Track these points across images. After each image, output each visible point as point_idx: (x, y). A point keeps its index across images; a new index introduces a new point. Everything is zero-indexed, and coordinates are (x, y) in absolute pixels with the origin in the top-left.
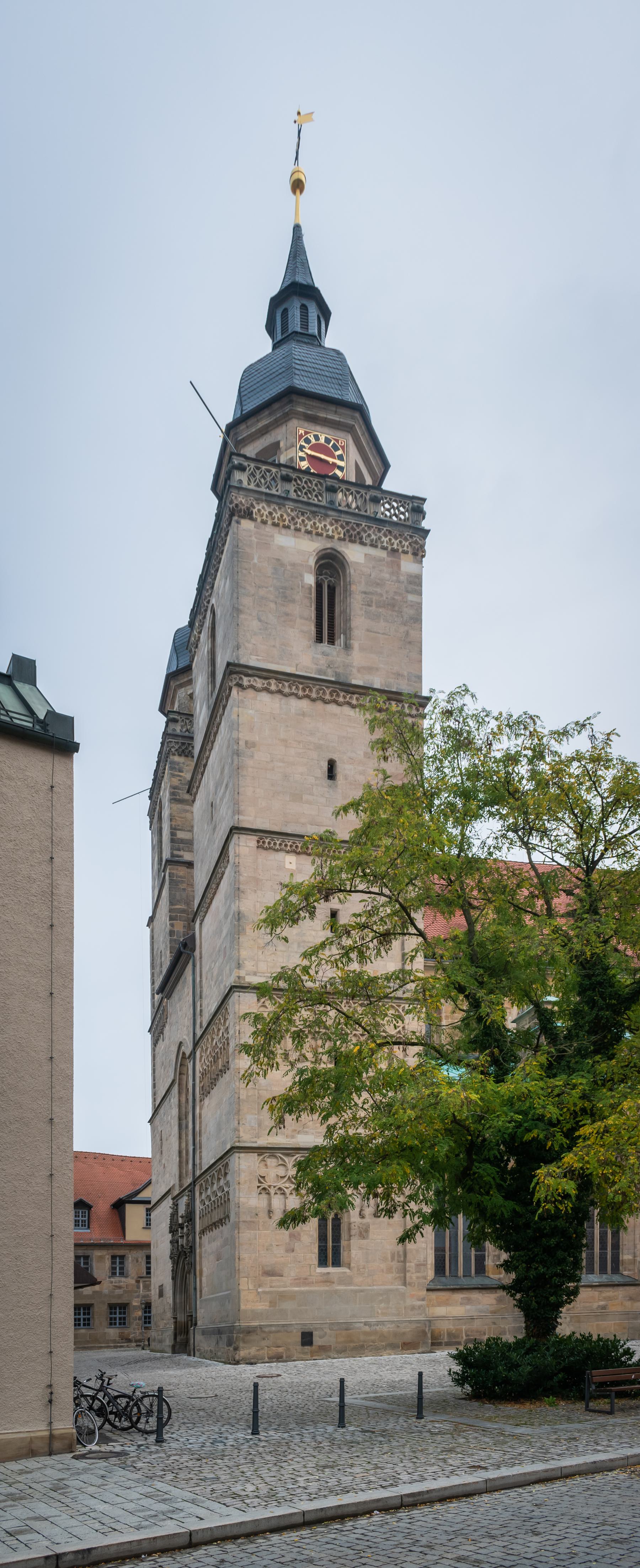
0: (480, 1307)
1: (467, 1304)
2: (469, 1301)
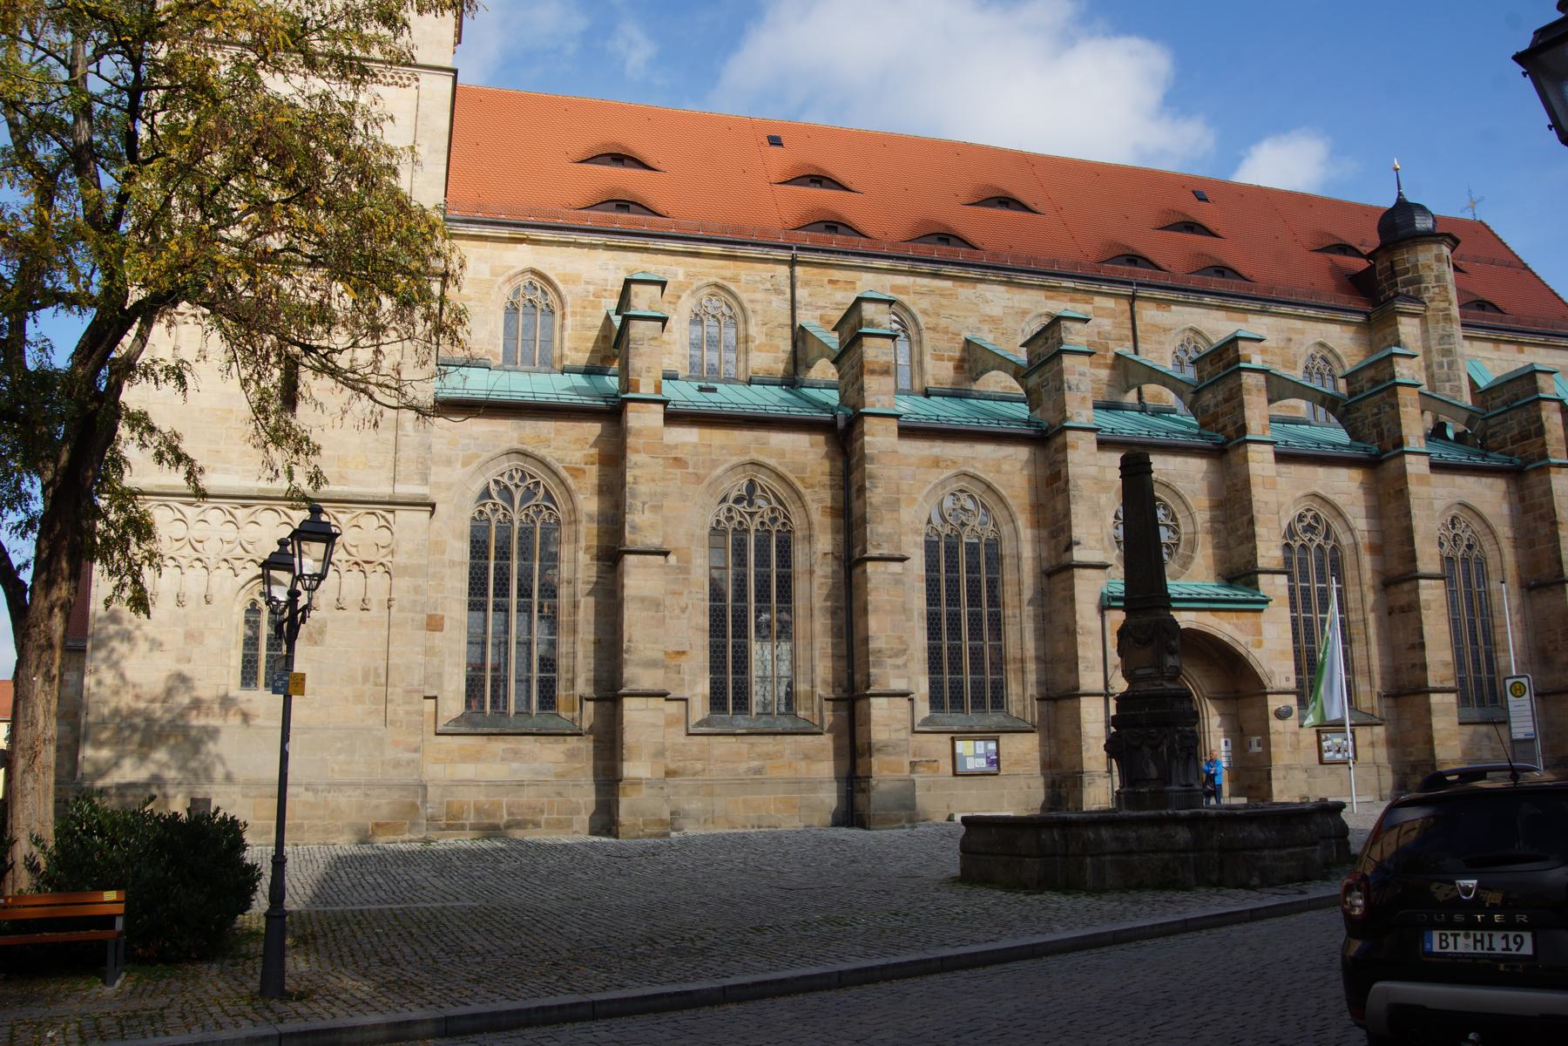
0: (537, 765)
1: (513, 760)
2: (516, 755)
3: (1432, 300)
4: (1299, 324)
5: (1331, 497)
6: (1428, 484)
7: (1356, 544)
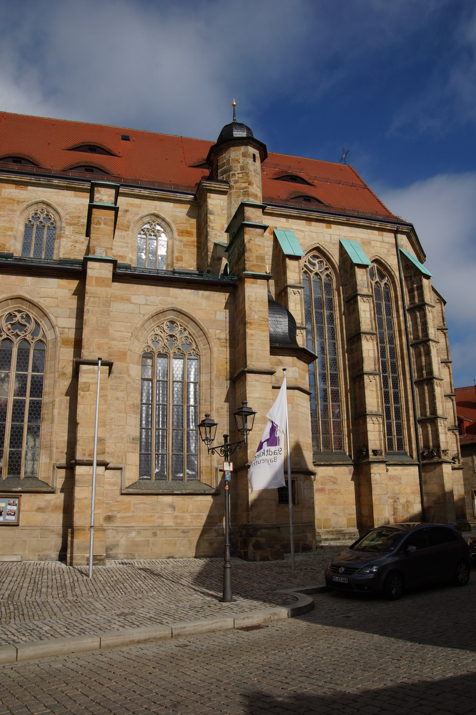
3: (236, 182)
4: (137, 201)
5: (36, 300)
6: (108, 286)
7: (56, 338)
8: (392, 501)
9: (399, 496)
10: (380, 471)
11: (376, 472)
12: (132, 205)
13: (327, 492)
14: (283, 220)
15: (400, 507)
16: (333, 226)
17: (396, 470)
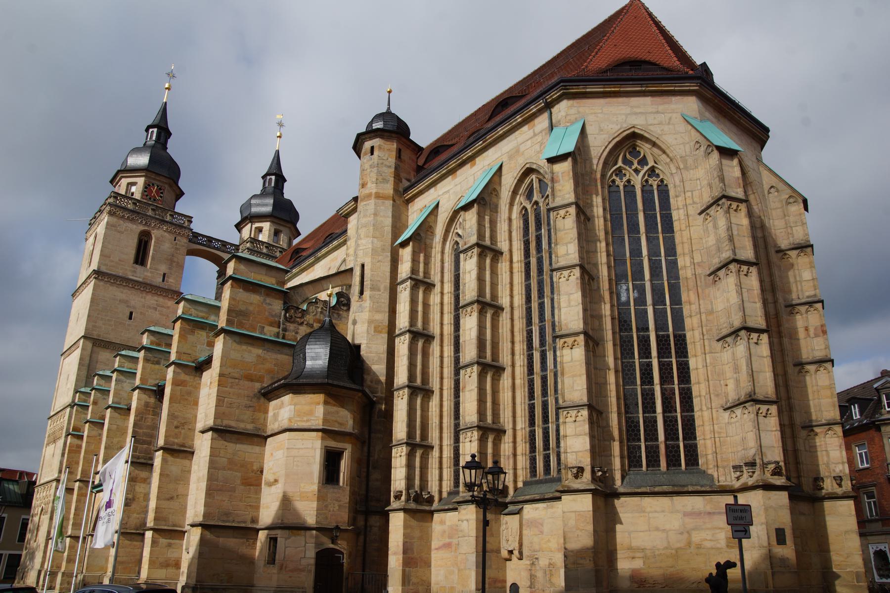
8: (528, 562)
9: (539, 554)
10: (467, 517)
11: (464, 518)
12: (332, 260)
13: (453, 548)
14: (432, 190)
15: (540, 574)
16: (477, 159)
17: (537, 509)
